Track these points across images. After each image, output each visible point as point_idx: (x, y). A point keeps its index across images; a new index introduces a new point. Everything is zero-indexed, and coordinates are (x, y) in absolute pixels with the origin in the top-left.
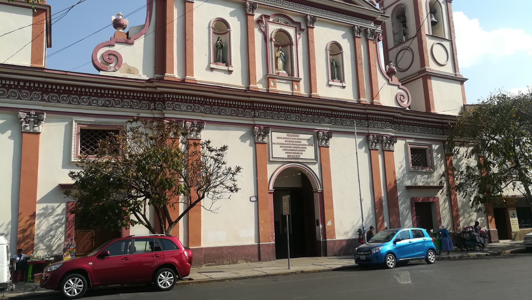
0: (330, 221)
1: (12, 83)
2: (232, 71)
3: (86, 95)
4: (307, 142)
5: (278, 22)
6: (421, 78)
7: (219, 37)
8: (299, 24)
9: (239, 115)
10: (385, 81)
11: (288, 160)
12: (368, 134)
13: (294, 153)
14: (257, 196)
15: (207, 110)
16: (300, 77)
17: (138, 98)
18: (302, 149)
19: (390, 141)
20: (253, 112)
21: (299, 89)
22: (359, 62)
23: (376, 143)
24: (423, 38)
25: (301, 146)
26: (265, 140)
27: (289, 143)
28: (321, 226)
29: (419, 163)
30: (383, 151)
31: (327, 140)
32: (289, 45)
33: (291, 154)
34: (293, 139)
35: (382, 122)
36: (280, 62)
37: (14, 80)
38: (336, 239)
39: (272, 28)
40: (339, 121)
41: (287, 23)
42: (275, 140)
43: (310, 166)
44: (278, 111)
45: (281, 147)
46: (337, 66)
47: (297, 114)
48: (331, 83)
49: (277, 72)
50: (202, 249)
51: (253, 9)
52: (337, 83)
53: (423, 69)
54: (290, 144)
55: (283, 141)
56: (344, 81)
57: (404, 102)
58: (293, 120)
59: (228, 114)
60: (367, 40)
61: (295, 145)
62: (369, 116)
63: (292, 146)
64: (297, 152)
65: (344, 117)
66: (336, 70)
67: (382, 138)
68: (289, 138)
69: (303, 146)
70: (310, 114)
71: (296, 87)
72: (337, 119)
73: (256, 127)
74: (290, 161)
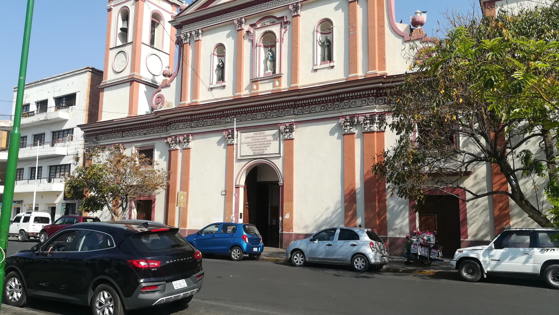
0: (288, 214)
3: (138, 129)
4: (272, 137)
11: (254, 157)
13: (259, 150)
16: (283, 72)
17: (162, 125)
21: (280, 85)
28: (280, 218)
33: (256, 152)
35: (363, 99)
36: (269, 63)
38: (293, 233)
39: (258, 34)
40: (306, 109)
41: (274, 22)
42: (244, 140)
43: (274, 161)
44: (245, 113)
47: (262, 112)
48: (315, 68)
50: (186, 230)
55: (250, 140)
56: (333, 60)
58: (259, 118)
62: (341, 96)
63: (258, 143)
64: (262, 148)
65: (312, 104)
66: (326, 49)
71: (277, 83)
72: (305, 107)
74: (256, 157)
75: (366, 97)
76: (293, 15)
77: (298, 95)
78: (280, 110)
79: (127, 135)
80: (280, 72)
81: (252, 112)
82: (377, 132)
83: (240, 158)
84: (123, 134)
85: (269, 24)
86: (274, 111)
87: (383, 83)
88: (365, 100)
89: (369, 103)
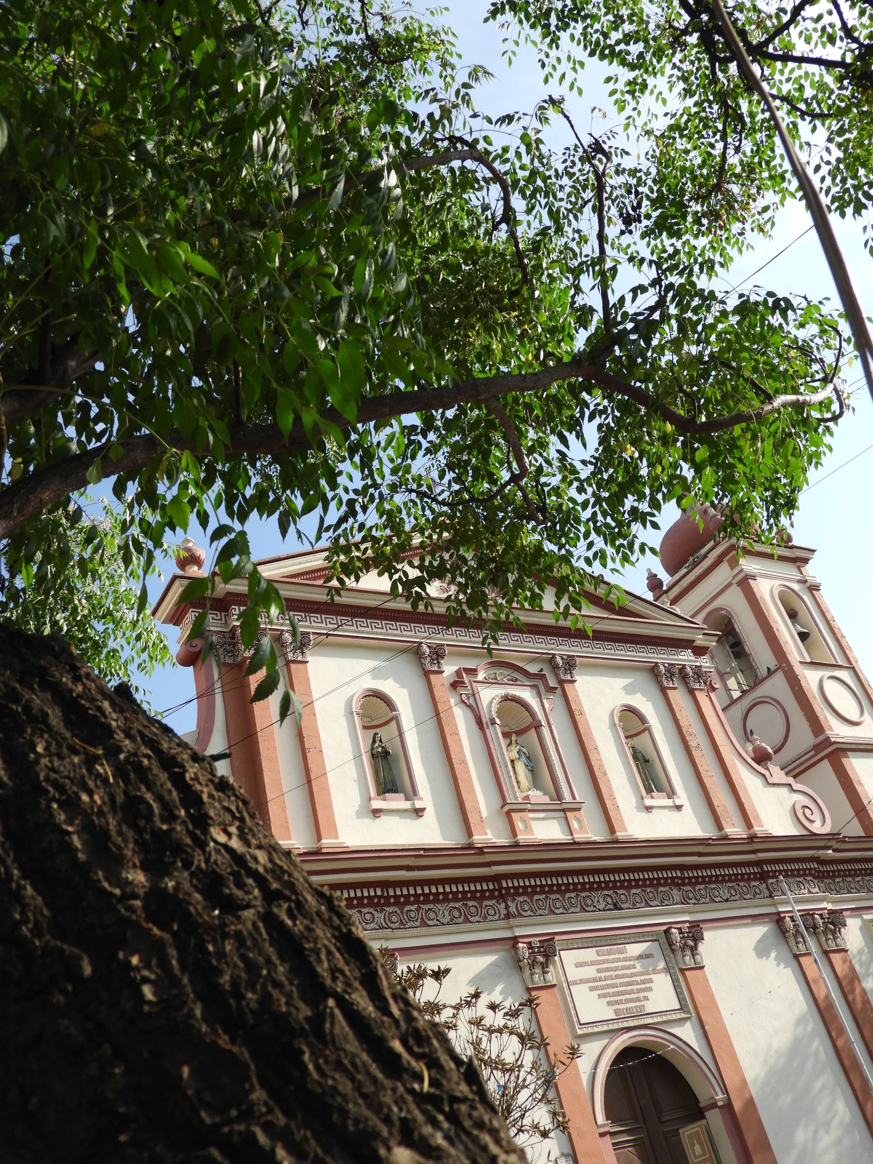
2: (423, 810)
6: (826, 762)
7: (376, 734)
8: (540, 676)
9: (472, 919)
10: (758, 781)
11: (621, 1025)
12: (776, 917)
13: (628, 1001)
14: (571, 1152)
15: (394, 919)
16: (578, 800)
18: (643, 986)
19: (832, 923)
20: (503, 905)
22: (692, 743)
24: (798, 669)
25: (638, 979)
26: (549, 977)
27: (607, 974)
30: (826, 953)
31: (694, 950)
32: (533, 732)
33: (622, 1006)
41: (516, 680)
44: (559, 891)
45: (592, 989)
46: (647, 761)
47: (606, 892)
48: (648, 802)
49: (523, 795)
51: (437, 659)
52: (659, 800)
53: (821, 738)
54: (611, 978)
55: (591, 972)
57: (813, 822)
58: (601, 907)
59: (445, 921)
60: (691, 692)
63: (618, 981)
64: (633, 996)
65: (710, 882)
67: (813, 919)
68: (604, 961)
70: (637, 886)
71: (575, 825)
73: (521, 945)
74: (626, 1025)
77: (700, 855)
78: (648, 890)
85: (506, 680)
86: (633, 891)
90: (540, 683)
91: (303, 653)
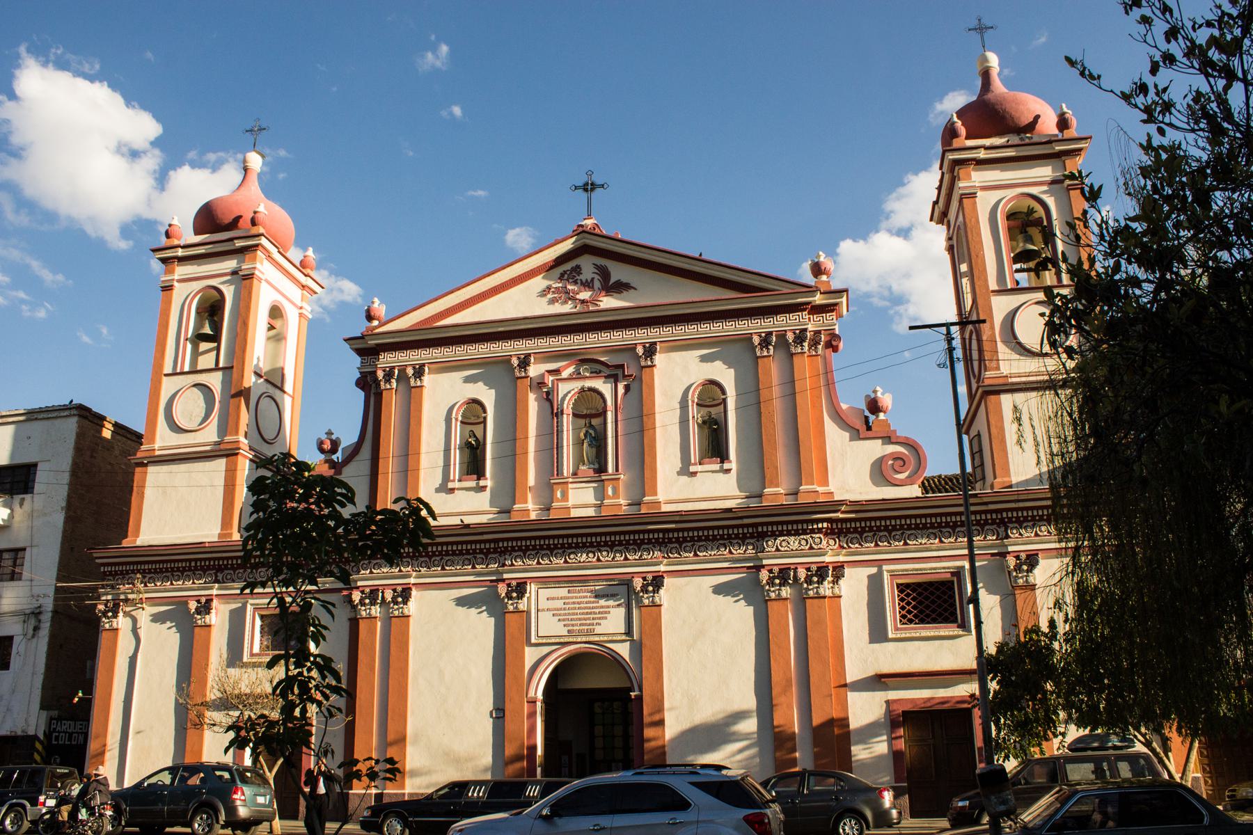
1: (184, 565)
2: (486, 487)
5: (579, 376)
11: (571, 640)
23: (780, 585)
25: (597, 611)
27: (572, 606)
29: (928, 616)
33: (575, 628)
34: (580, 597)
35: (802, 537)
37: (186, 560)
39: (567, 391)
41: (600, 372)
42: (544, 604)
48: (692, 469)
54: (575, 609)
55: (559, 604)
61: (585, 608)
62: (760, 529)
63: (579, 611)
64: (588, 622)
68: (572, 598)
69: (602, 610)
70: (617, 545)
74: (575, 640)
75: (808, 534)
76: (643, 363)
79: (229, 577)
80: (617, 470)
81: (565, 548)
82: (830, 597)
83: (536, 641)
84: (216, 576)
85: (588, 375)
87: (843, 512)
88: (807, 541)
89: (813, 545)
90: (619, 372)
91: (421, 380)
